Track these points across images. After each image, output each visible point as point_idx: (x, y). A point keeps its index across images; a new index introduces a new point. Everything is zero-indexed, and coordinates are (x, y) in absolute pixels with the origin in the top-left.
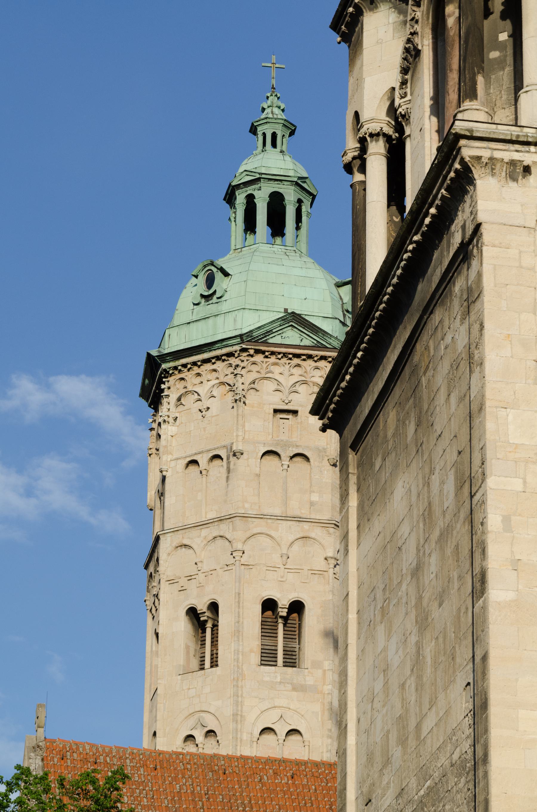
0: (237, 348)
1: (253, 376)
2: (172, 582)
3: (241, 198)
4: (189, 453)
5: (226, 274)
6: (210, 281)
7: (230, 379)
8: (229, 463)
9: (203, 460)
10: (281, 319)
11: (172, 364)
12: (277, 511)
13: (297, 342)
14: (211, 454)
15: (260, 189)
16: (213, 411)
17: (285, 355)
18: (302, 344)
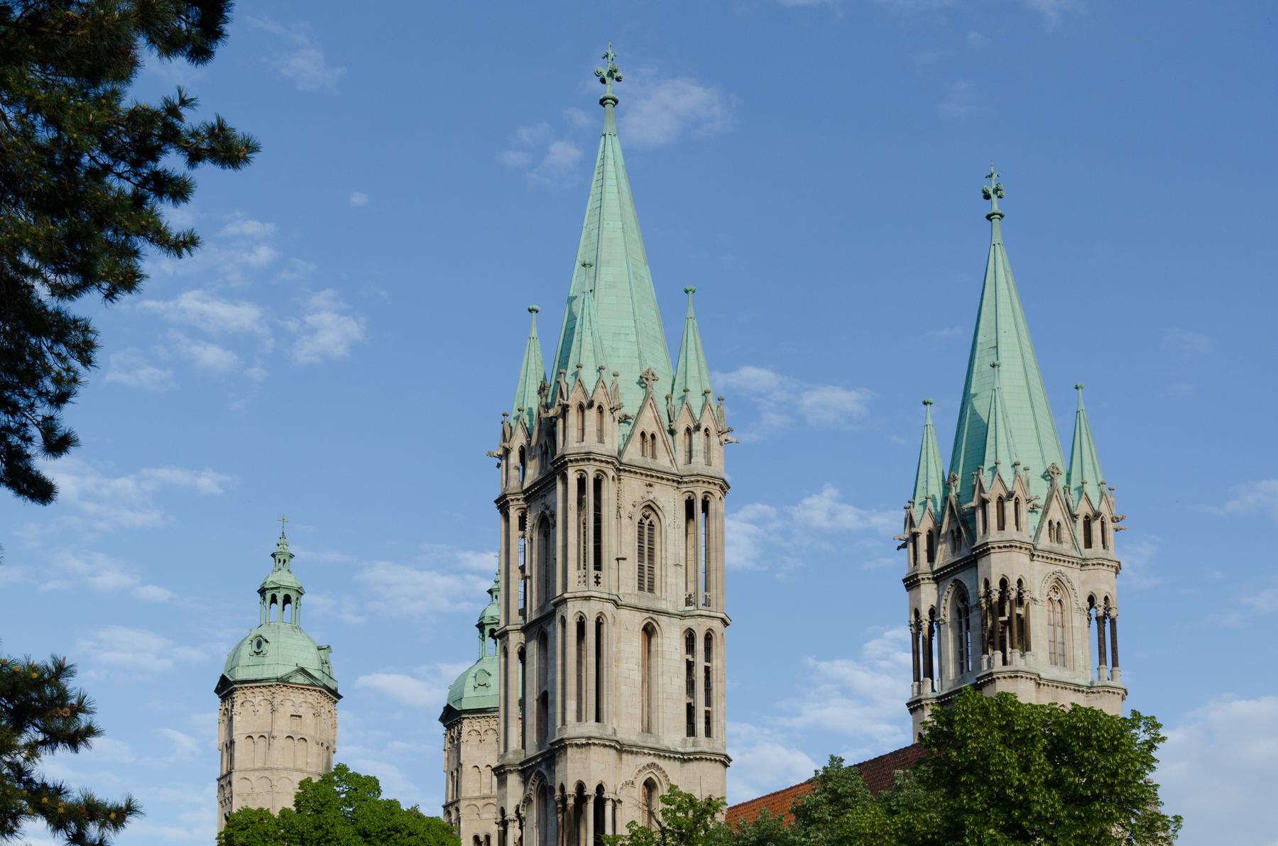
0: (275, 683)
1: (281, 698)
2: (239, 795)
3: (268, 595)
4: (248, 731)
5: (267, 641)
6: (259, 645)
7: (270, 698)
8: (269, 741)
9: (256, 737)
10: (297, 671)
11: (240, 686)
12: (291, 766)
13: (302, 682)
14: (260, 735)
15: (279, 592)
16: (261, 712)
17: (297, 688)
18: (305, 683)
